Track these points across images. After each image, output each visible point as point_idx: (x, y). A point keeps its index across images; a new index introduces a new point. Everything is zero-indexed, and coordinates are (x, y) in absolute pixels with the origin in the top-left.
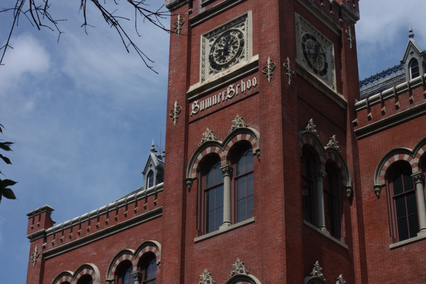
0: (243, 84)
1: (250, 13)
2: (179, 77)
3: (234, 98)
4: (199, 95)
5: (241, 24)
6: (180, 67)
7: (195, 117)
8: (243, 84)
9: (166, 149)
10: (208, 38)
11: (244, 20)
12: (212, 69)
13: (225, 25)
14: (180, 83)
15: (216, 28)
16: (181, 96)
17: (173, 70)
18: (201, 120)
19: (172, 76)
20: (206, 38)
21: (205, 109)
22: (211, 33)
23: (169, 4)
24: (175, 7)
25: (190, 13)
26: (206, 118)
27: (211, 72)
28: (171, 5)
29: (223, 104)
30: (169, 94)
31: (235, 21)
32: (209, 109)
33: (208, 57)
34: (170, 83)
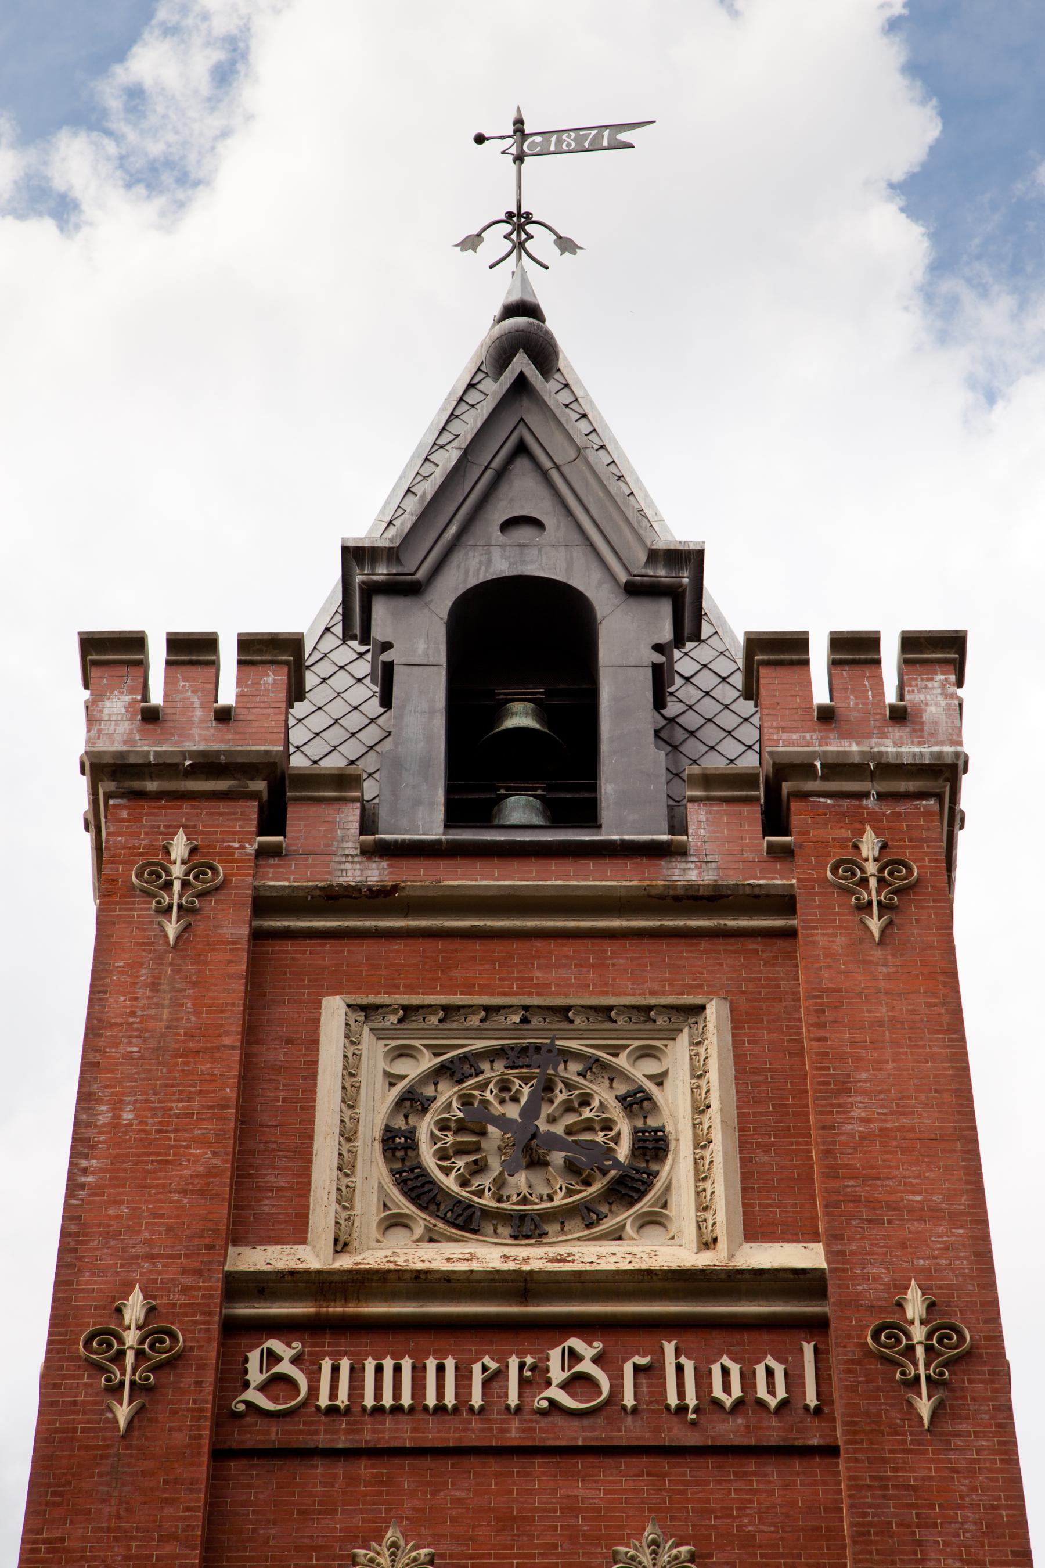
0: (680, 1369)
1: (715, 1012)
2: (167, 1162)
3: (600, 1421)
4: (317, 1316)
5: (637, 1043)
6: (177, 1108)
7: (274, 1435)
8: (680, 1369)
9: (33, 1551)
10: (379, 1034)
11: (672, 1035)
12: (407, 1207)
13: (526, 1008)
14: (176, 1197)
15: (458, 999)
16: (185, 1272)
17: (116, 1110)
18: (320, 1468)
19: (102, 1138)
20: (366, 1029)
21: (356, 1409)
22: (409, 1011)
23: (121, 754)
24: (152, 786)
25: (264, 853)
26: (364, 1468)
27: (394, 1222)
28: (132, 760)
29: (508, 1430)
30: (73, 1228)
31: (605, 1012)
32: (389, 1422)
33: (378, 1134)
34: (85, 1171)
